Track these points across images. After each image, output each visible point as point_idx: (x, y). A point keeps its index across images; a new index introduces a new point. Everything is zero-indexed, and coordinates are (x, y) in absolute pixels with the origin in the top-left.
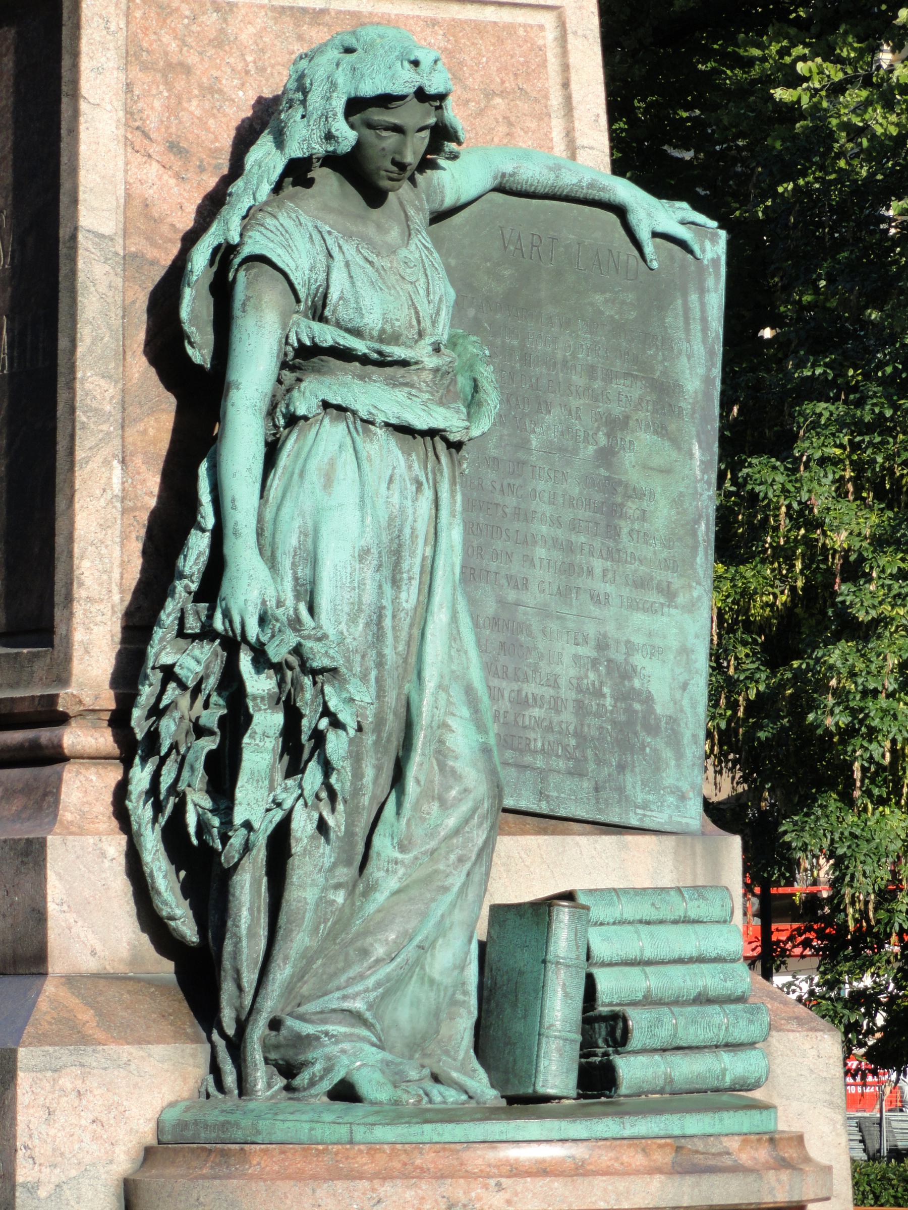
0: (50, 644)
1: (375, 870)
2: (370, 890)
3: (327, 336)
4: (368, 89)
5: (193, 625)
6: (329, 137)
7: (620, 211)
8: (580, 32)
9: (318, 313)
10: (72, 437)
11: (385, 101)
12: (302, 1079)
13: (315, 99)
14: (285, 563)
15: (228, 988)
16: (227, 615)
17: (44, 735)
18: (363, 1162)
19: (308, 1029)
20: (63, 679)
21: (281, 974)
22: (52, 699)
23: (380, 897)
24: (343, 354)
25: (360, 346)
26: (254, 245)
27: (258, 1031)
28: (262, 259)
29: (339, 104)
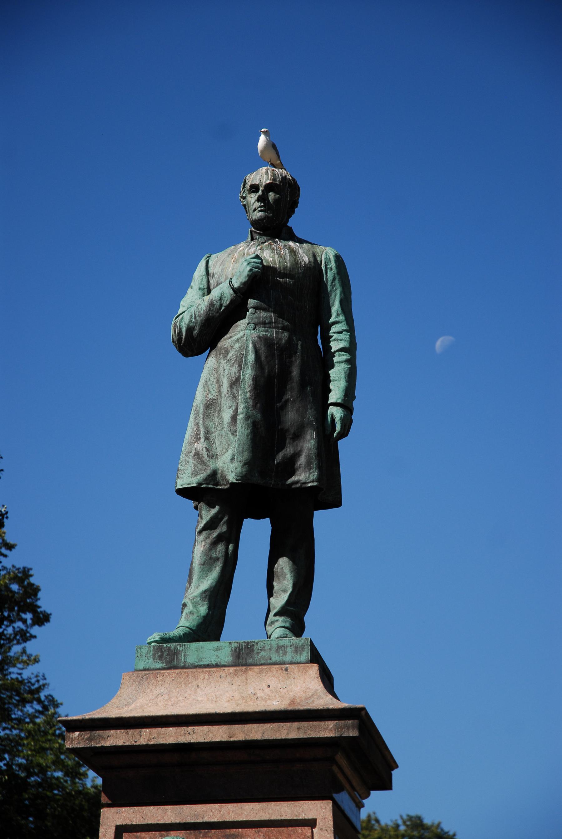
8: (324, 829)
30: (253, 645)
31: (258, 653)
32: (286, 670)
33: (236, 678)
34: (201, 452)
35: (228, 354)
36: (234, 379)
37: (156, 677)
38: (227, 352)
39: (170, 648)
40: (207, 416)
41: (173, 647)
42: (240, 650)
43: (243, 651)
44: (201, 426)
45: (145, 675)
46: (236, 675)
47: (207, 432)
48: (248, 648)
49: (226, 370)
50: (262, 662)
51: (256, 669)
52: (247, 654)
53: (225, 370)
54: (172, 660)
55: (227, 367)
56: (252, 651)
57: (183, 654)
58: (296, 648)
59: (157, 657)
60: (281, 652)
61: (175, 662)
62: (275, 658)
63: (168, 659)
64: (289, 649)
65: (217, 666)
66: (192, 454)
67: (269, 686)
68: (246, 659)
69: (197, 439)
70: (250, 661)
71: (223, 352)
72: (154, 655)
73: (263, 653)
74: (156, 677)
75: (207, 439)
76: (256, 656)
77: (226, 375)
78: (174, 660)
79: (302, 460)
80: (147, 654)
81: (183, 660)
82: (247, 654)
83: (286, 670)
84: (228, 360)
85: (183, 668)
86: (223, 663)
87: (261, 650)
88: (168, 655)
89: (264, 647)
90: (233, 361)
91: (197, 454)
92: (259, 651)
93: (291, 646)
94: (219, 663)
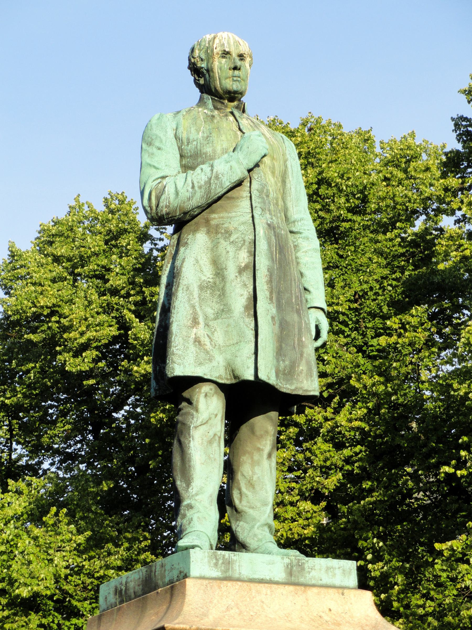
30: (304, 563)
31: (309, 573)
32: (343, 594)
33: (296, 596)
34: (202, 339)
35: (230, 235)
36: (243, 265)
37: (220, 587)
38: (228, 233)
39: (224, 556)
40: (203, 299)
41: (227, 556)
42: (292, 567)
43: (294, 568)
44: (198, 309)
45: (209, 583)
46: (296, 594)
47: (206, 318)
48: (299, 565)
49: (230, 253)
50: (314, 582)
51: (315, 590)
52: (299, 572)
53: (228, 252)
54: (227, 570)
55: (231, 249)
56: (303, 569)
57: (237, 564)
58: (344, 571)
59: (212, 565)
60: (330, 574)
61: (230, 572)
62: (326, 580)
63: (223, 568)
64: (337, 571)
65: (270, 582)
66: (191, 340)
67: (330, 610)
68: (298, 577)
69: (195, 322)
70: (302, 580)
71: (223, 231)
72: (209, 562)
73: (313, 573)
74: (220, 587)
75: (207, 325)
76: (307, 575)
77: (231, 258)
78: (229, 569)
79: (303, 367)
80: (202, 559)
81: (238, 571)
82: (299, 572)
83: (343, 594)
84: (232, 242)
85: (239, 580)
86: (276, 579)
87: (312, 569)
88: (223, 563)
89: (314, 566)
90: (240, 245)
91: (197, 341)
92: (310, 570)
93: (339, 568)
94: (272, 579)
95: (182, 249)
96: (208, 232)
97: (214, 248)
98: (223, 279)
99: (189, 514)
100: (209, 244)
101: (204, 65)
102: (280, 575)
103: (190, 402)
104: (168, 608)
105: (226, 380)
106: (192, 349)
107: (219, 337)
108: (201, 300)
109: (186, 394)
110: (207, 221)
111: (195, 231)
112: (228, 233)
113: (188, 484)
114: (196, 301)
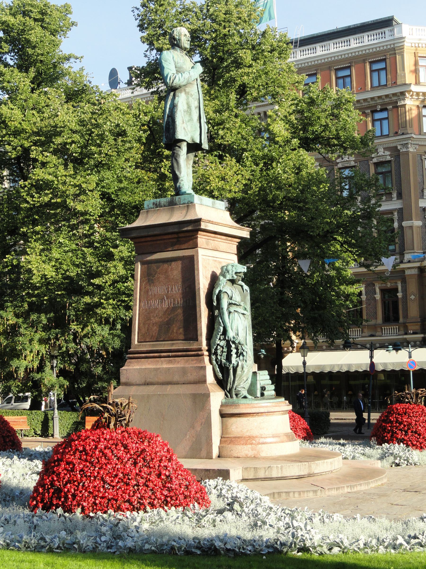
0: (197, 341)
1: (244, 369)
2: (244, 372)
3: (234, 302)
4: (238, 271)
5: (222, 338)
6: (233, 277)
7: (242, 286)
9: (231, 299)
10: (201, 314)
11: (240, 273)
12: (239, 396)
13: (230, 272)
14: (234, 330)
15: (229, 384)
16: (228, 337)
17: (200, 353)
18: (256, 406)
19: (239, 389)
20: (202, 346)
21: (236, 382)
22: (201, 348)
23: (245, 372)
24: (235, 304)
25: (237, 303)
26: (224, 290)
27: (233, 390)
28: (226, 292)
29: (234, 273)
55: (193, 100)
69: (183, 122)
95: (177, 98)
96: (185, 93)
97: (188, 99)
98: (191, 109)
99: (182, 182)
100: (186, 98)
101: (177, 37)
102: (211, 205)
103: (180, 147)
104: (187, 212)
105: (190, 142)
106: (183, 131)
107: (189, 127)
108: (184, 115)
109: (178, 144)
110: (185, 90)
111: (181, 92)
112: (192, 95)
113: (180, 173)
114: (183, 115)
